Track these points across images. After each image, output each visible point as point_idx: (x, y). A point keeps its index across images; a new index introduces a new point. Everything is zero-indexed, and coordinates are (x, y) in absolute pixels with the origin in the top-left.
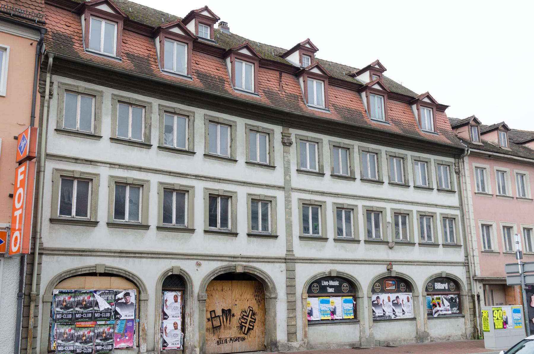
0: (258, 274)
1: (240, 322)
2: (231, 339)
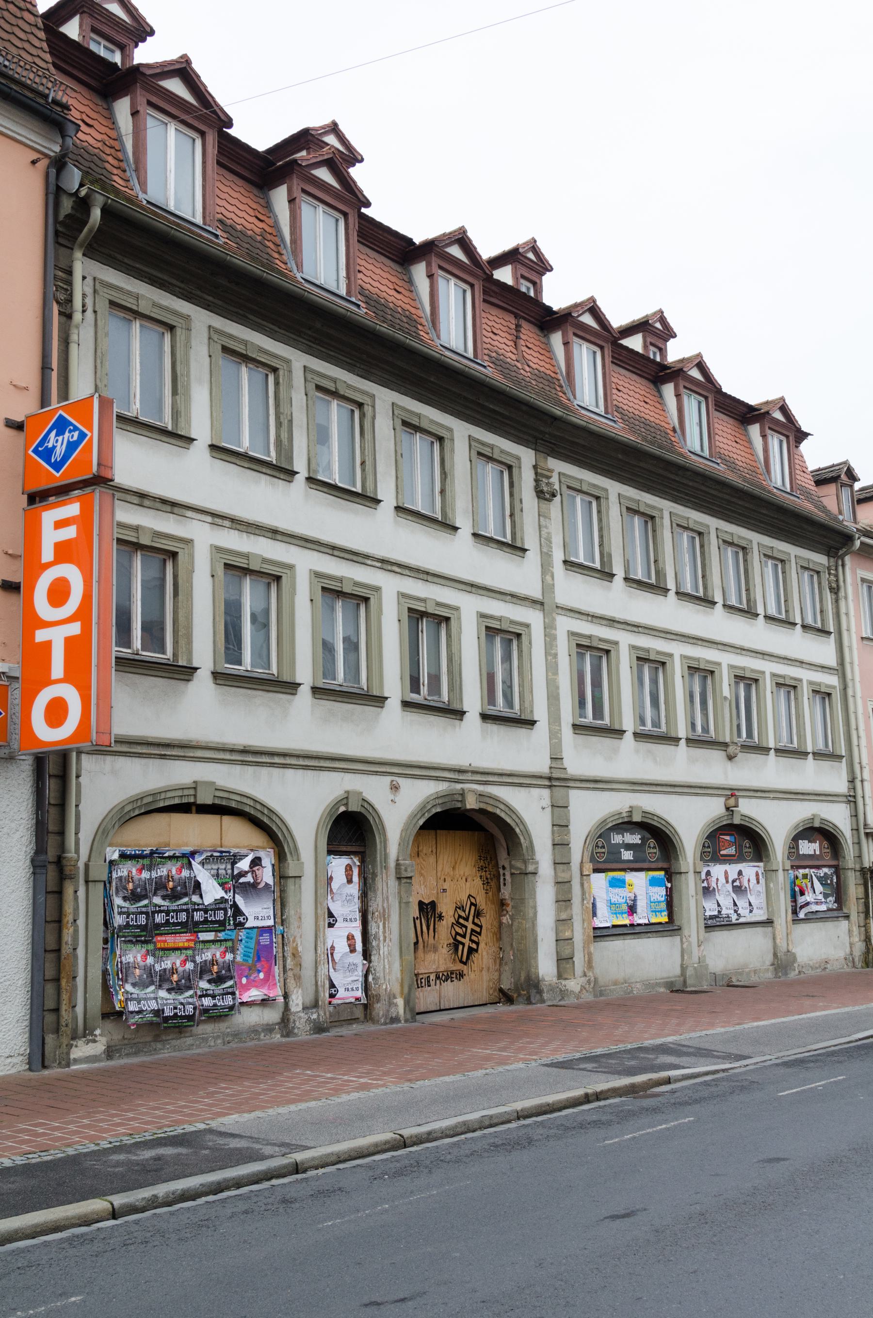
0: (503, 815)
1: (453, 933)
2: (438, 977)
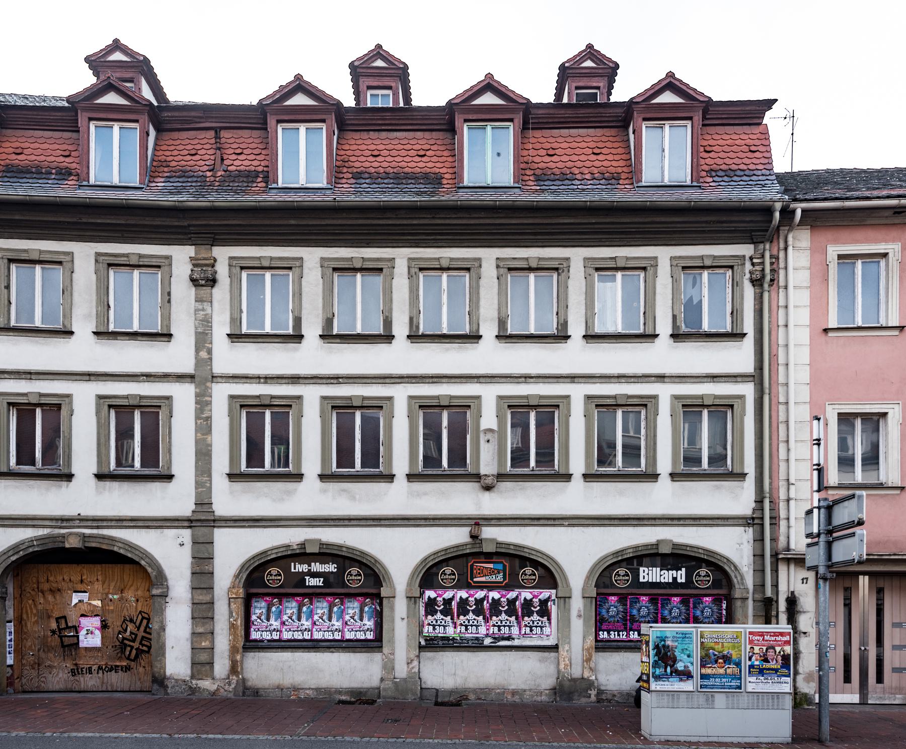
0: (122, 551)
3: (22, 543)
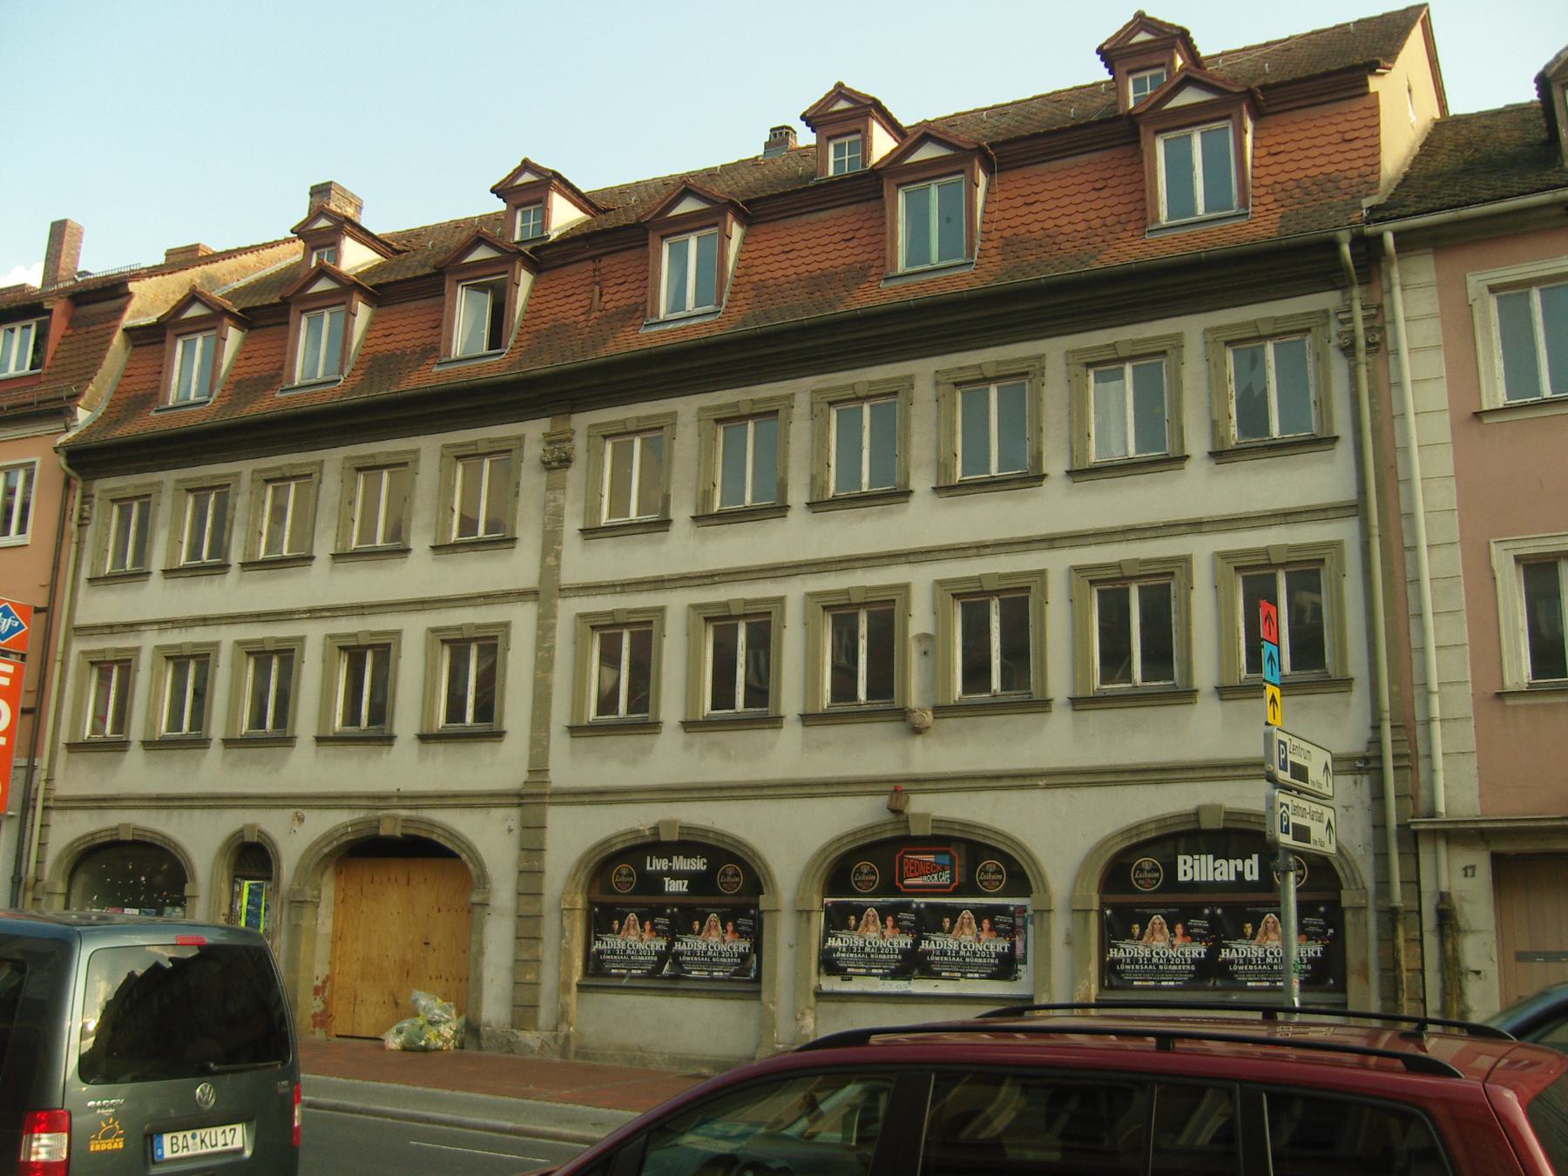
3: (336, 829)
